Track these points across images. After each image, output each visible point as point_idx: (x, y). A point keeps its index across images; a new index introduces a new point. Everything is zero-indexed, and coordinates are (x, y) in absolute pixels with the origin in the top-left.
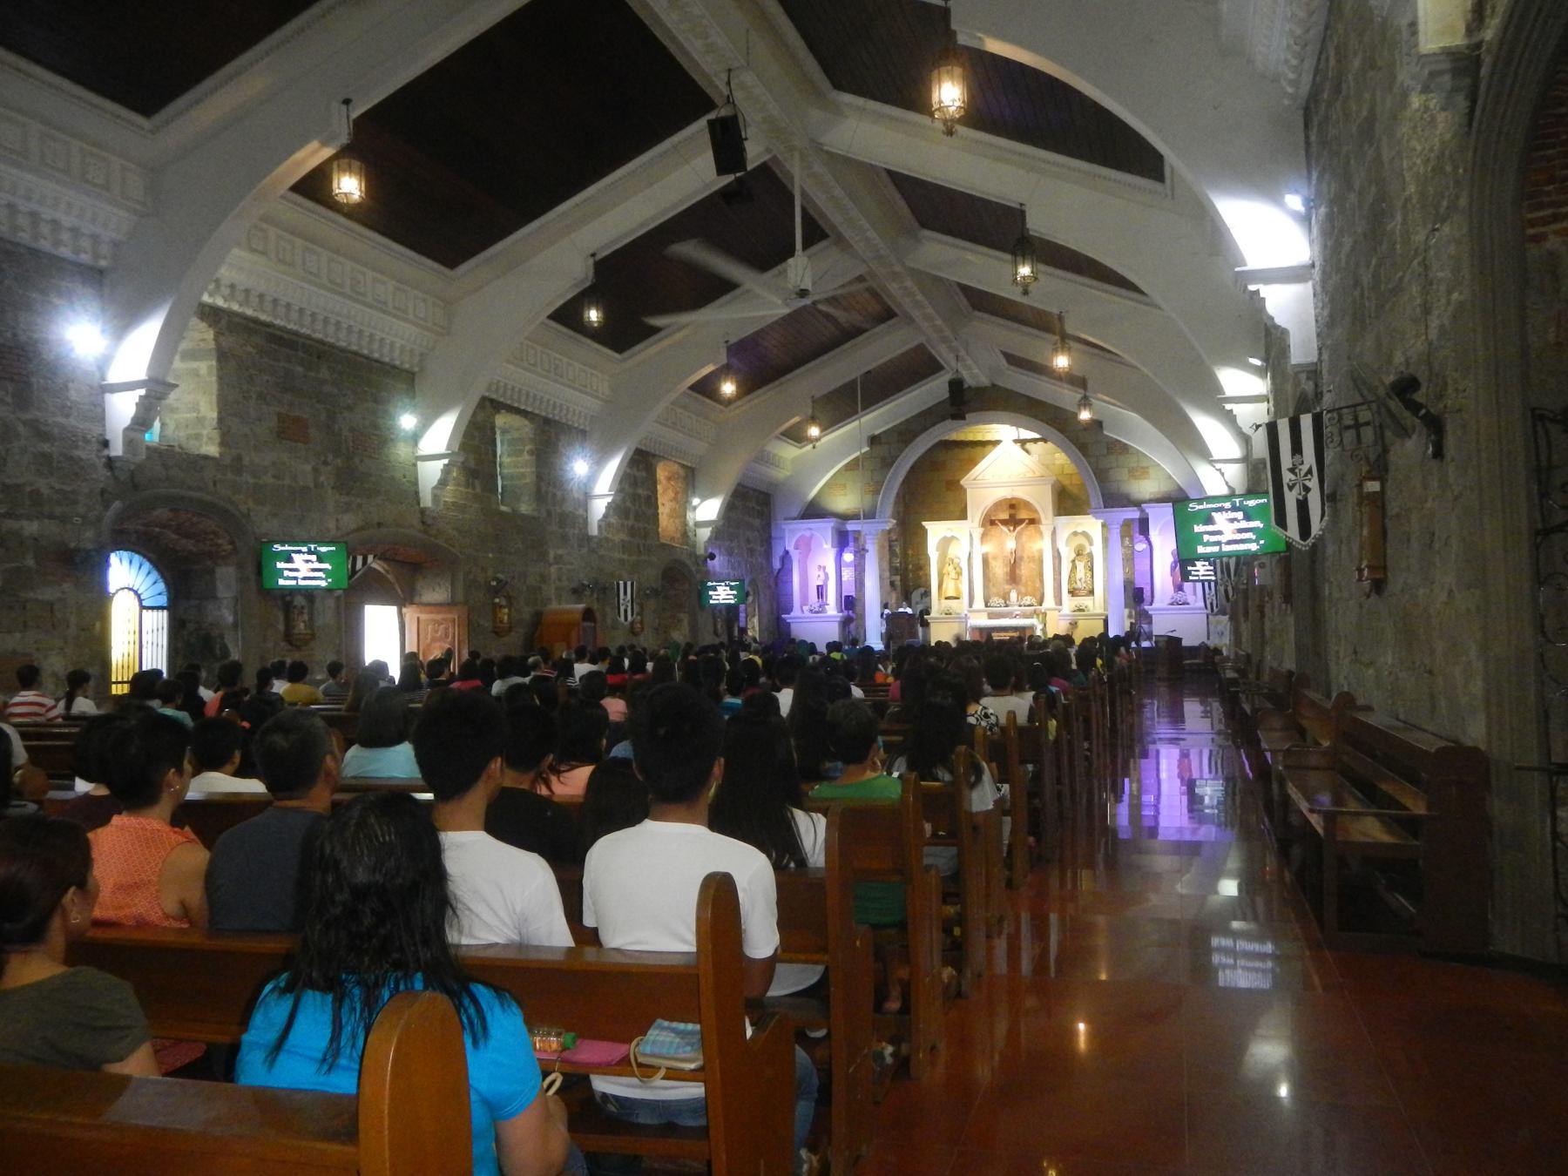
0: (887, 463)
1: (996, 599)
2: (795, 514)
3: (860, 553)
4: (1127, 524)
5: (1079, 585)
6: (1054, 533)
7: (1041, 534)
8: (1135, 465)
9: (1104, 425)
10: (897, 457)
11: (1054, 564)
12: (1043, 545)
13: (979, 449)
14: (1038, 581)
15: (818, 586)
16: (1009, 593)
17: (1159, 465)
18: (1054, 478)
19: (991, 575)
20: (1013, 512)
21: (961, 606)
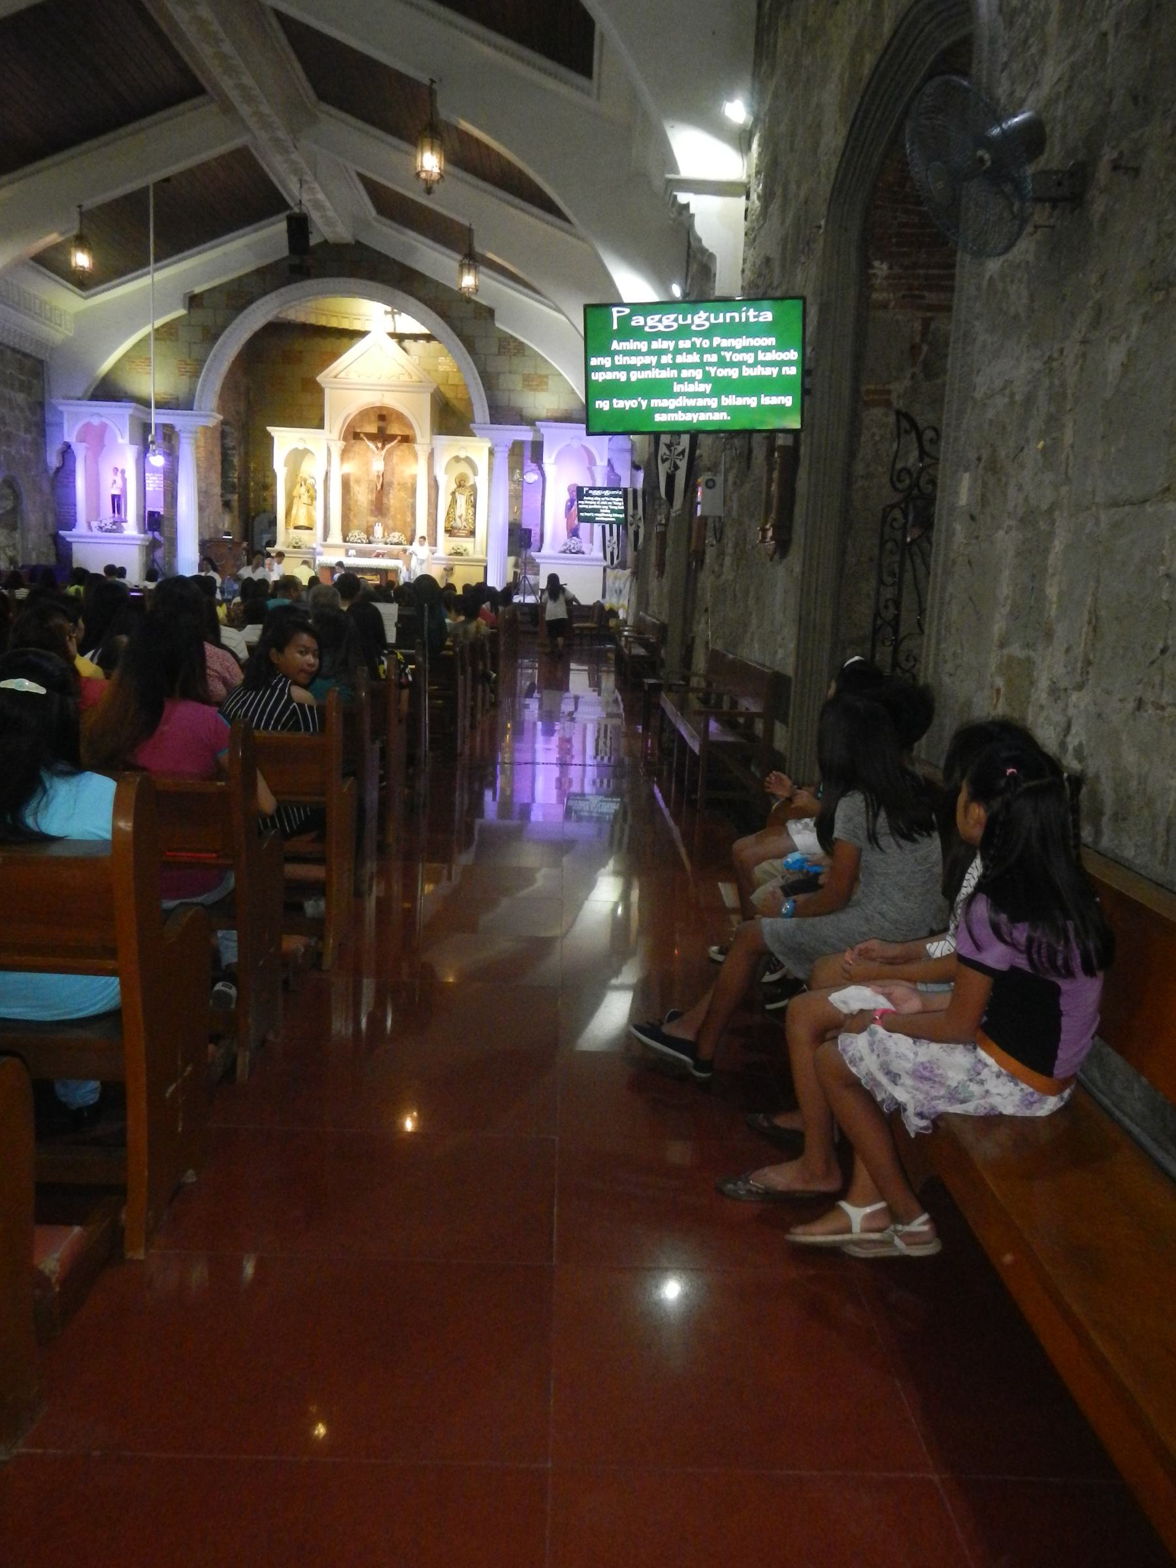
0: (211, 336)
1: (356, 533)
2: (80, 395)
3: (172, 455)
4: (517, 449)
5: (459, 523)
6: (431, 456)
7: (416, 456)
8: (532, 372)
9: (497, 315)
10: (224, 328)
11: (429, 495)
12: (417, 470)
13: (345, 340)
14: (409, 514)
15: (114, 497)
16: (372, 527)
17: (560, 375)
18: (435, 386)
19: (352, 502)
20: (382, 424)
21: (312, 539)
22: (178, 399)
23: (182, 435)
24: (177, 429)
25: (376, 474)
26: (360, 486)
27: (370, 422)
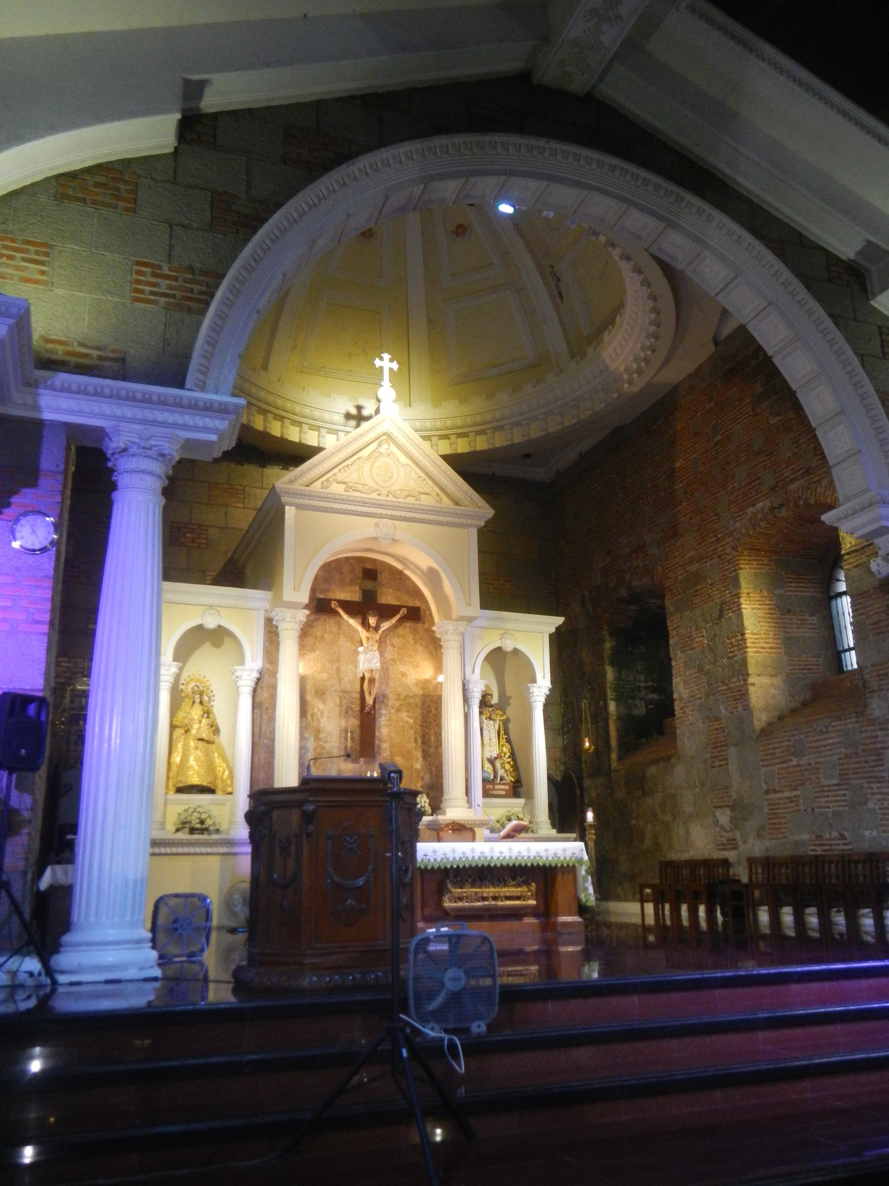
7: (434, 647)
14: (419, 754)
20: (369, 585)
22: (123, 360)
23: (123, 464)
24: (115, 443)
25: (367, 676)
26: (324, 702)
27: (342, 584)
